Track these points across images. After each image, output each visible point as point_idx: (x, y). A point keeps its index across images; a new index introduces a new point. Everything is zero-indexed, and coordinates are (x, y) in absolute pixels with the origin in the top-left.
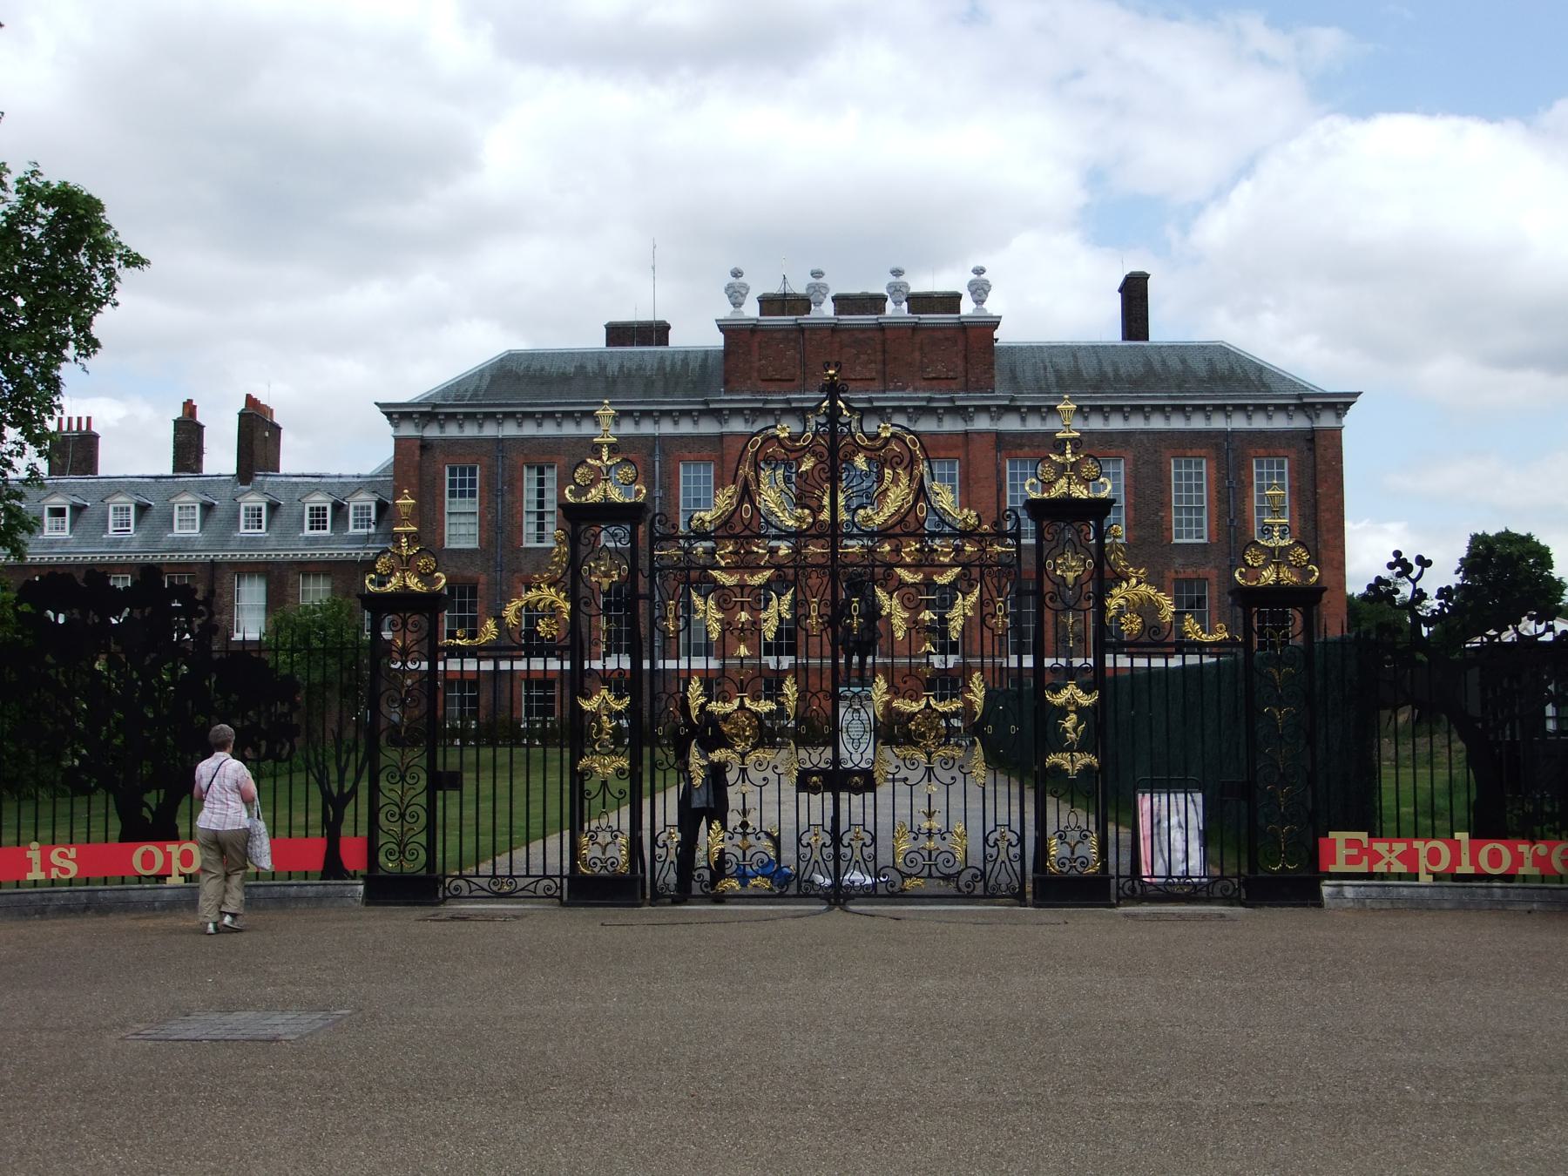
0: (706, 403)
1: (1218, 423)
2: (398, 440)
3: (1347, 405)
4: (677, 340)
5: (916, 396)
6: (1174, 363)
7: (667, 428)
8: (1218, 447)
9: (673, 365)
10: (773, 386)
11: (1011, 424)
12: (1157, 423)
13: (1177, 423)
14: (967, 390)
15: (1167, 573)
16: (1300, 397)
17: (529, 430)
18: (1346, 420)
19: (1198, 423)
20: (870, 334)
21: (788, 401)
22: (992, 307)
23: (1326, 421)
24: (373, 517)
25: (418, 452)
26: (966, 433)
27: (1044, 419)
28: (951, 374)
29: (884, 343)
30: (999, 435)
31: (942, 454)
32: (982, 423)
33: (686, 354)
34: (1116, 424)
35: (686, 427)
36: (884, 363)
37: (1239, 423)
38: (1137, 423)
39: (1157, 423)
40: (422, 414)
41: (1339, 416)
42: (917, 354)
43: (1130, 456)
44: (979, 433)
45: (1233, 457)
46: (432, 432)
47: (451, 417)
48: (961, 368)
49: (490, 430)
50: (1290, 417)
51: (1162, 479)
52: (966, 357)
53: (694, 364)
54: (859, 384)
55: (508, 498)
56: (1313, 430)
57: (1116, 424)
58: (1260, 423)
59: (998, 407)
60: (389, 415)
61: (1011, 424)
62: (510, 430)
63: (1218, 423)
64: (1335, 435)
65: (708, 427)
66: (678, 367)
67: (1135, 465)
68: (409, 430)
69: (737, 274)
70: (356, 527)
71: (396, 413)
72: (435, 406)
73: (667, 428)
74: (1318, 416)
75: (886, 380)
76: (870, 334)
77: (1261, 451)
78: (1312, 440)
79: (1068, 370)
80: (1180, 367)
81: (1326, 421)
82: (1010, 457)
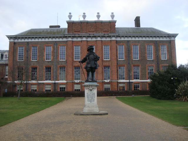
0: (64, 35)
1: (154, 39)
2: (10, 42)
3: (176, 36)
4: (61, 27)
5: (101, 34)
6: (145, 30)
7: (57, 40)
8: (154, 43)
9: (59, 31)
10: (76, 33)
11: (119, 39)
12: (144, 39)
13: (147, 39)
14: (111, 33)
15: (146, 65)
16: (168, 34)
17: (33, 40)
18: (176, 39)
19: (151, 39)
20: (93, 24)
21: (79, 35)
22: (115, 19)
23: (172, 39)
24: (8, 56)
25: (13, 44)
26: (111, 41)
27: (124, 38)
28: (108, 30)
29: (96, 25)
30: (116, 41)
31: (106, 44)
32: (114, 39)
33: (62, 29)
34: (137, 39)
35: (61, 40)
36: (96, 28)
37: (158, 39)
38: (140, 39)
39: (144, 39)
40: (14, 38)
41: (175, 38)
42: (102, 27)
43: (139, 45)
44: (113, 40)
45: (157, 44)
46: (16, 41)
47: (19, 38)
48: (110, 29)
49: (26, 40)
50: (166, 38)
51: (145, 48)
52: (110, 28)
53: (63, 31)
54: (91, 32)
55: (29, 52)
56: (170, 40)
57: (137, 39)
58: (161, 39)
59: (117, 36)
60: (8, 38)
61: (119, 39)
62: (30, 40)
63: (154, 39)
64: (174, 41)
65: (65, 40)
66: (60, 31)
67: (140, 46)
68: (12, 40)
69: (70, 13)
70: (5, 58)
71: (10, 37)
72: (16, 36)
73: (57, 40)
74: (171, 38)
75: (96, 31)
76: (93, 24)
77: (162, 44)
78: (170, 42)
79: (127, 33)
80: (146, 31)
81: (172, 39)
82: (119, 45)
